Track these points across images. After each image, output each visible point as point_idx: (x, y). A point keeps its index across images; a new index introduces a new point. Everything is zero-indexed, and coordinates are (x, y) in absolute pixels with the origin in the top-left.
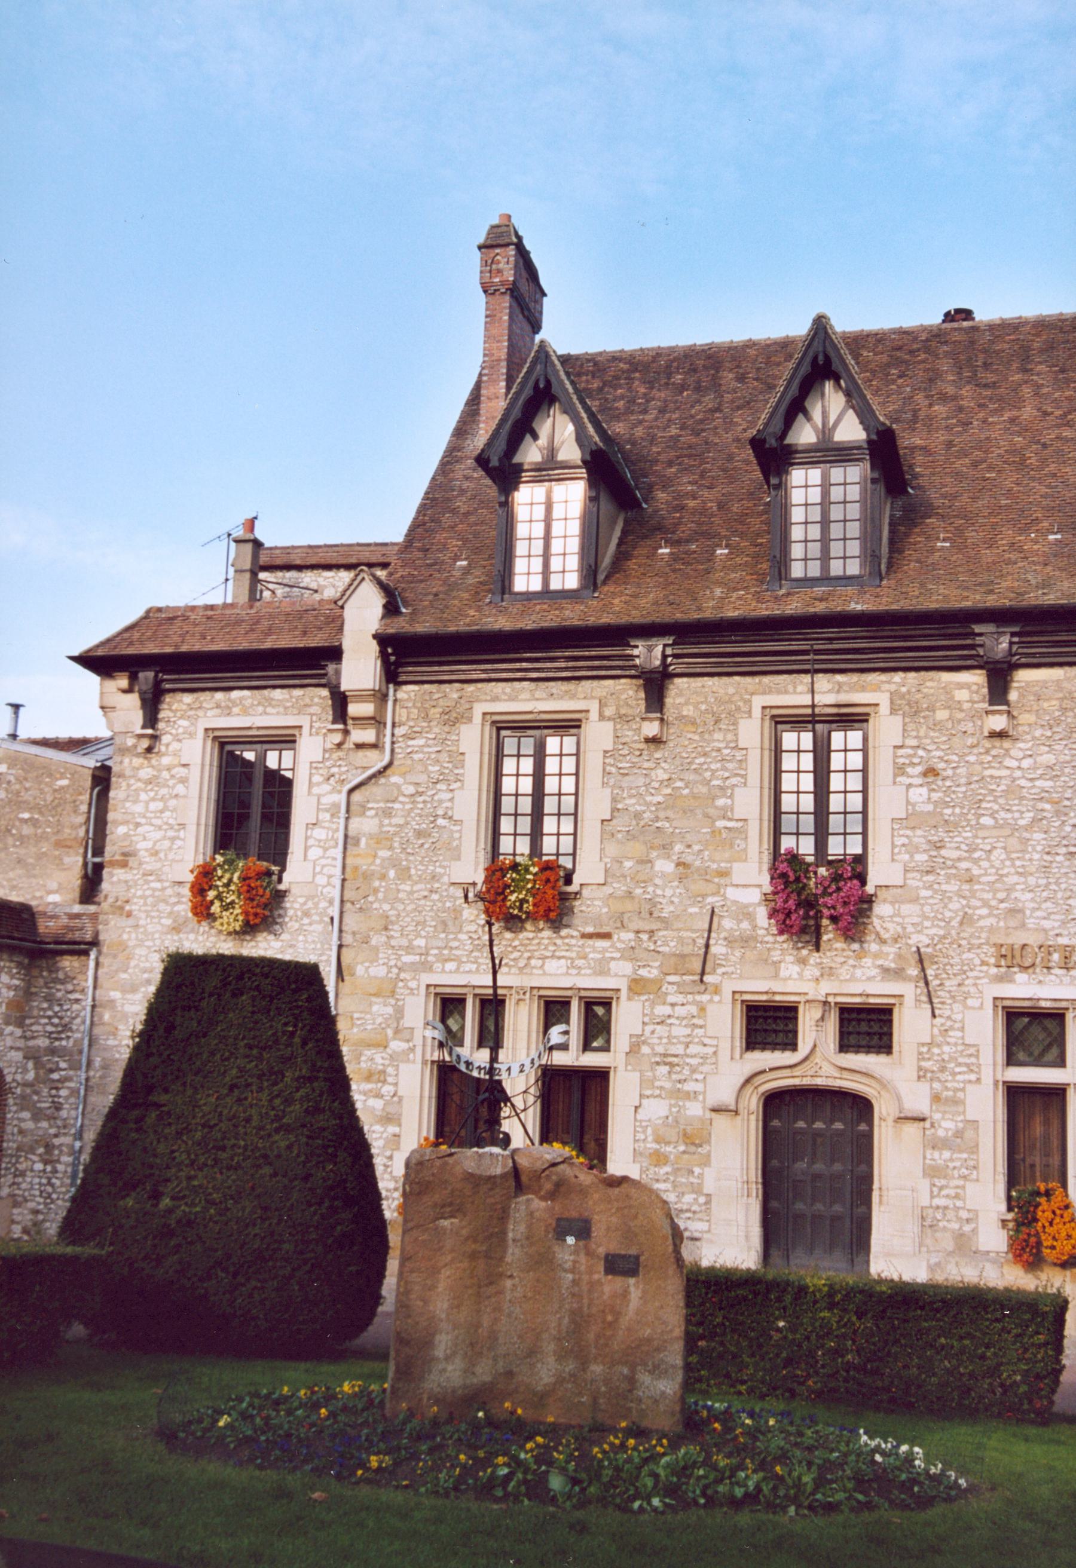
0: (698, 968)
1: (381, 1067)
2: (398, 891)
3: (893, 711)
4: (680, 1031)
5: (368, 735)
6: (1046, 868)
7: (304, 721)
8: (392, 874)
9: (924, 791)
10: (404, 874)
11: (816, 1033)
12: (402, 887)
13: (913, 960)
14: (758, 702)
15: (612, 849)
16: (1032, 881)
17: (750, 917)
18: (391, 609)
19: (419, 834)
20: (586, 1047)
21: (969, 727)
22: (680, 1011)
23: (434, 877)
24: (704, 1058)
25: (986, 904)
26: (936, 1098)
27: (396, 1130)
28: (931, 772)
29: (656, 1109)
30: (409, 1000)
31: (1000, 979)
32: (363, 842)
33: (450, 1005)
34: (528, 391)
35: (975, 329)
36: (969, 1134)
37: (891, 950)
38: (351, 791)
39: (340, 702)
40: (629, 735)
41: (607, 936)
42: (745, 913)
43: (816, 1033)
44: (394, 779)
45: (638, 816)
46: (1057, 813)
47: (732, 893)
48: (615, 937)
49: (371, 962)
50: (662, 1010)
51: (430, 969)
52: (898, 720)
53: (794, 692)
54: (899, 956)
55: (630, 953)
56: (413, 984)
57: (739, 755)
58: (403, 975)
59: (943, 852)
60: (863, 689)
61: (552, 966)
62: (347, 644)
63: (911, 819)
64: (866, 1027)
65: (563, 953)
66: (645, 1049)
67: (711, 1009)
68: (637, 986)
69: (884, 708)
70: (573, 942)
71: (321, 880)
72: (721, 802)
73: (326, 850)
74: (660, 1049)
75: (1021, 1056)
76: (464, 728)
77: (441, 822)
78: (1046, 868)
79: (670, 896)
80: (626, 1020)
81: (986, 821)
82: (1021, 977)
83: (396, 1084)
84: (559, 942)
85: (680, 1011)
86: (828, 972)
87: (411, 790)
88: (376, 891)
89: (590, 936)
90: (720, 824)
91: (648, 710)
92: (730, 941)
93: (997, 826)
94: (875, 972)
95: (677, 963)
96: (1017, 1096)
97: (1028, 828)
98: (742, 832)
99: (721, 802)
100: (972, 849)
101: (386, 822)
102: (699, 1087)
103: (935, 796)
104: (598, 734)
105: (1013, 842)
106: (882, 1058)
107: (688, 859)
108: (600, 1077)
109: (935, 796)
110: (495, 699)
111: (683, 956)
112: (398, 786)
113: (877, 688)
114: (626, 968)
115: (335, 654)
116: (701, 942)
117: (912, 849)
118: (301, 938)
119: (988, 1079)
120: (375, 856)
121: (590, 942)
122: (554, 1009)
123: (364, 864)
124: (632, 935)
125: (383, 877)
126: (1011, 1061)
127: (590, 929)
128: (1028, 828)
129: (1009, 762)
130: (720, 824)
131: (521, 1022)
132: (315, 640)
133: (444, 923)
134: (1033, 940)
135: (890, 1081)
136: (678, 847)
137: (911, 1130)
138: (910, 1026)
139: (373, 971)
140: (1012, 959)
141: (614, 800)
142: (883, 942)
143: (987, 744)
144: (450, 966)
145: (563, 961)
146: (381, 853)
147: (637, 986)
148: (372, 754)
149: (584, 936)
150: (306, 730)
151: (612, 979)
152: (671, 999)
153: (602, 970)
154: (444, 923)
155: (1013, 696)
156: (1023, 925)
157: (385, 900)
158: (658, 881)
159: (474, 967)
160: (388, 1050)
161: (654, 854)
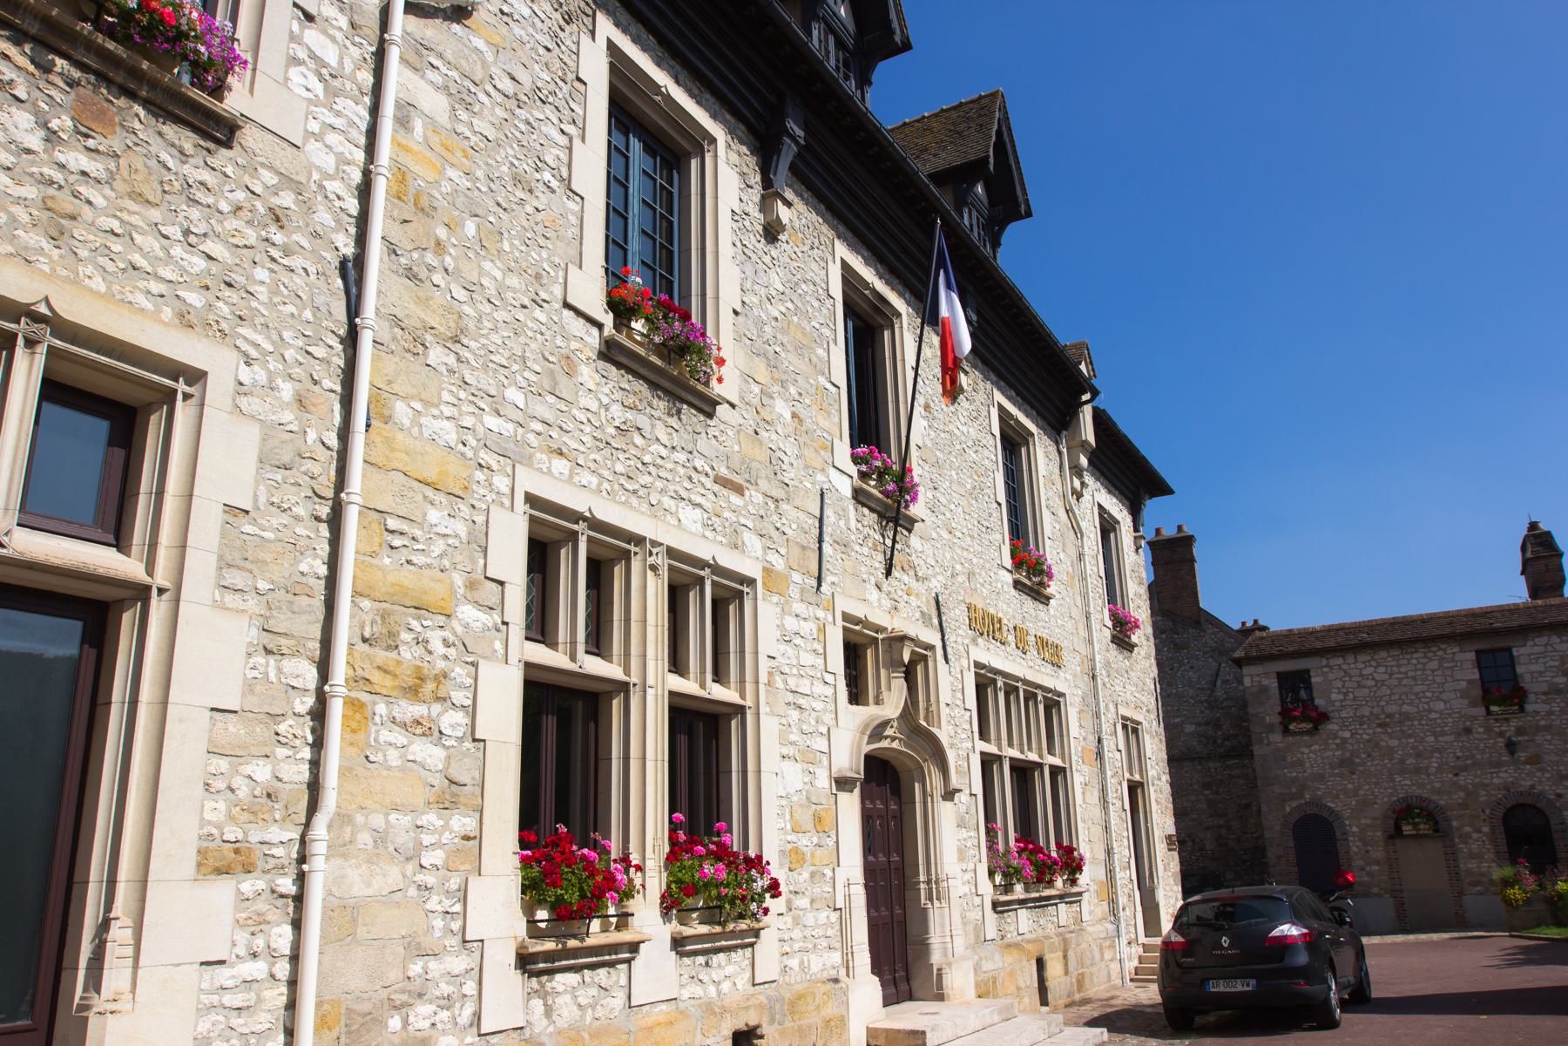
1: (441, 665)
8: (470, 228)
12: (487, 265)
19: (517, 180)
30: (496, 512)
32: (418, 125)
41: (739, 490)
48: (747, 493)
51: (528, 461)
58: (487, 457)
61: (690, 516)
65: (699, 499)
73: (333, 94)
74: (792, 682)
77: (547, 176)
83: (472, 711)
84: (694, 475)
94: (918, 615)
101: (463, 115)
102: (821, 744)
107: (799, 408)
118: (261, 274)
120: (442, 172)
121: (725, 492)
123: (422, 172)
127: (723, 471)
139: (431, 424)
144: (560, 465)
145: (698, 511)
146: (451, 173)
149: (719, 480)
159: (594, 480)
160: (455, 623)
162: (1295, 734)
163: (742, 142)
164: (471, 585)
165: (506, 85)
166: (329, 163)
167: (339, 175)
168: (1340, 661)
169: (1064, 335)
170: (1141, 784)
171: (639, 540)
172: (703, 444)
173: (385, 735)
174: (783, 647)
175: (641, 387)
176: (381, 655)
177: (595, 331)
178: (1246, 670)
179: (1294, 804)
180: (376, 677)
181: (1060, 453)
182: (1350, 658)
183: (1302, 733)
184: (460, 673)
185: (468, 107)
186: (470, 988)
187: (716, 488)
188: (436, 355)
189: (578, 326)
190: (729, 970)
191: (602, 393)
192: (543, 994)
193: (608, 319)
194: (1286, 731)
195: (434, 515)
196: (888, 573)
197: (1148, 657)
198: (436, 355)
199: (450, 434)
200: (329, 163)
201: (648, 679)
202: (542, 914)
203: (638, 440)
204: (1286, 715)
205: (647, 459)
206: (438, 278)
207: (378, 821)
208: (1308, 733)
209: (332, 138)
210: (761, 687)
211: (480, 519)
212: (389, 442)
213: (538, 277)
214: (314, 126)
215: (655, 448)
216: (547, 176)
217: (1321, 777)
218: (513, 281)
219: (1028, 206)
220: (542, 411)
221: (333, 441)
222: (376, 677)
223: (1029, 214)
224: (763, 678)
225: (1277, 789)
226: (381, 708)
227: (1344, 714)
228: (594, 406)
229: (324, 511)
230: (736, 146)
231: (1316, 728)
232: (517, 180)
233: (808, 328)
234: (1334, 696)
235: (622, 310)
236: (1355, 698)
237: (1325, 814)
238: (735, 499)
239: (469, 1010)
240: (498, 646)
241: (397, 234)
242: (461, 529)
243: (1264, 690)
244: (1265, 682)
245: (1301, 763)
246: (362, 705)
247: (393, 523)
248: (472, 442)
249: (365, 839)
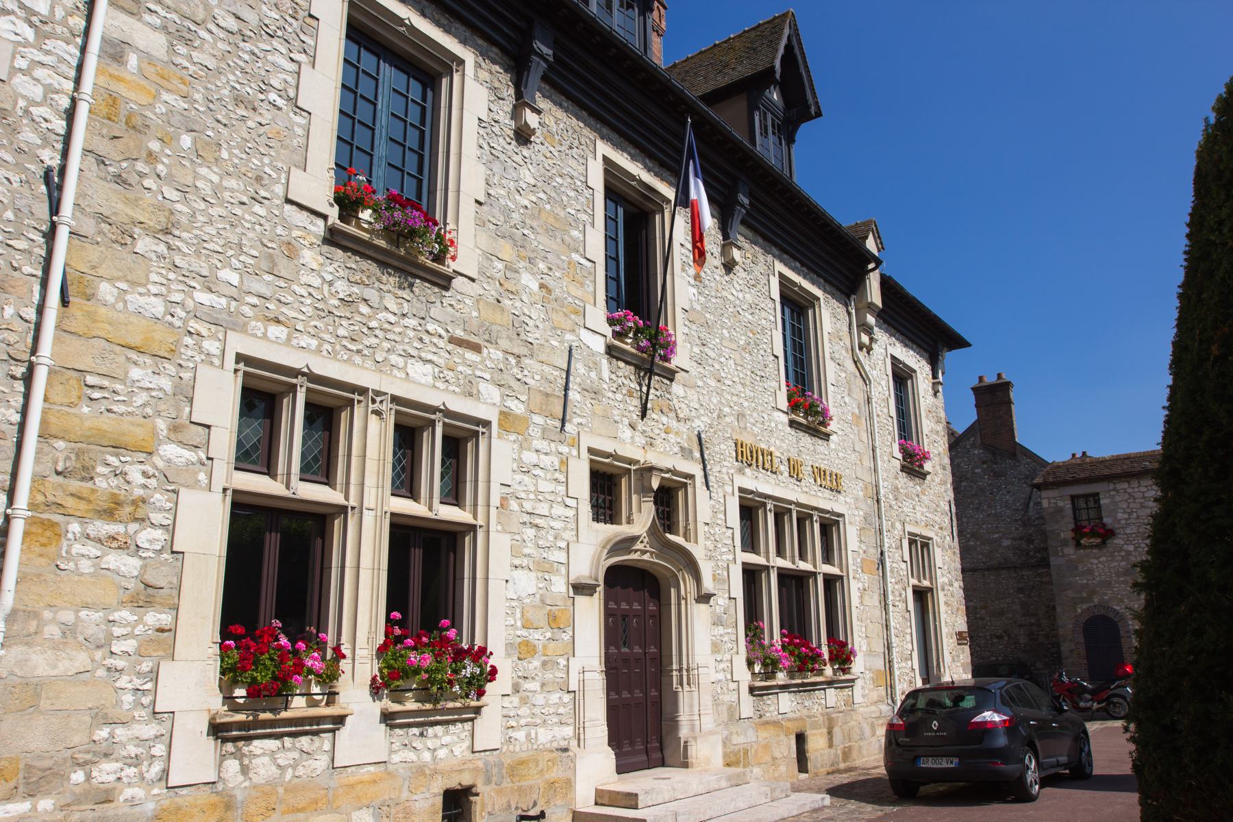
1: (139, 492)
2: (196, 176)
8: (186, 141)
9: (695, 291)
10: (205, 152)
12: (203, 171)
17: (596, 366)
19: (239, 100)
22: (546, 461)
23: (259, 179)
27: (166, 619)
30: (203, 370)
32: (133, 60)
33: (261, 398)
41: (477, 348)
45: (507, 212)
48: (485, 351)
49: (133, 283)
51: (243, 329)
56: (212, 346)
58: (194, 325)
59: (706, 350)
61: (418, 370)
65: (430, 357)
70: (441, 343)
74: (528, 506)
77: (273, 96)
80: (499, 460)
83: (171, 529)
84: (426, 338)
85: (546, 461)
89: (460, 342)
94: (676, 449)
99: (575, 233)
101: (182, 49)
102: (562, 557)
107: (549, 281)
120: (156, 97)
121: (460, 350)
123: (133, 99)
124: (500, 355)
127: (459, 333)
131: (370, 440)
144: (275, 331)
145: (429, 366)
146: (166, 96)
149: (453, 340)
157: (169, 179)
158: (525, 298)
159: (314, 343)
160: (156, 460)
161: (522, 264)
162: (1085, 547)
163: (494, 62)
164: (175, 429)
165: (232, 24)
166: (37, 92)
167: (45, 101)
168: (1126, 485)
169: (844, 216)
170: (931, 590)
171: (363, 391)
172: (435, 311)
173: (77, 548)
174: (519, 477)
175: (373, 267)
176: (74, 485)
177: (320, 222)
178: (1045, 494)
179: (1085, 606)
180: (70, 502)
181: (849, 314)
182: (1135, 483)
183: (1092, 547)
184: (159, 498)
185: (188, 42)
186: (159, 750)
187: (450, 347)
188: (144, 244)
189: (302, 218)
190: (447, 739)
191: (323, 272)
192: (238, 755)
193: (333, 213)
194: (1078, 545)
195: (135, 373)
196: (643, 415)
197: (943, 483)
198: (144, 244)
199: (158, 308)
200: (37, 92)
201: (368, 503)
202: (240, 692)
203: (364, 309)
204: (1078, 531)
205: (373, 324)
206: (147, 183)
207: (68, 616)
208: (1097, 546)
209: (39, 73)
210: (493, 511)
211: (187, 375)
212: (92, 317)
213: (259, 179)
214: (21, 63)
215: (382, 315)
216: (273, 96)
217: (1108, 584)
218: (232, 183)
219: (818, 107)
220: (257, 287)
221: (31, 314)
222: (70, 502)
223: (819, 114)
224: (495, 501)
225: (1070, 594)
226: (75, 527)
227: (1128, 531)
228: (316, 282)
229: (20, 370)
230: (486, 65)
231: (1104, 543)
232: (239, 100)
233: (562, 214)
234: (1120, 515)
235: (348, 204)
236: (1138, 517)
237: (1111, 615)
238: (471, 356)
239: (157, 768)
240: (202, 477)
241: (104, 147)
242: (166, 384)
243: (1060, 510)
244: (1061, 504)
245: (1090, 572)
246: (53, 525)
247: (91, 380)
248: (180, 312)
249: (52, 631)
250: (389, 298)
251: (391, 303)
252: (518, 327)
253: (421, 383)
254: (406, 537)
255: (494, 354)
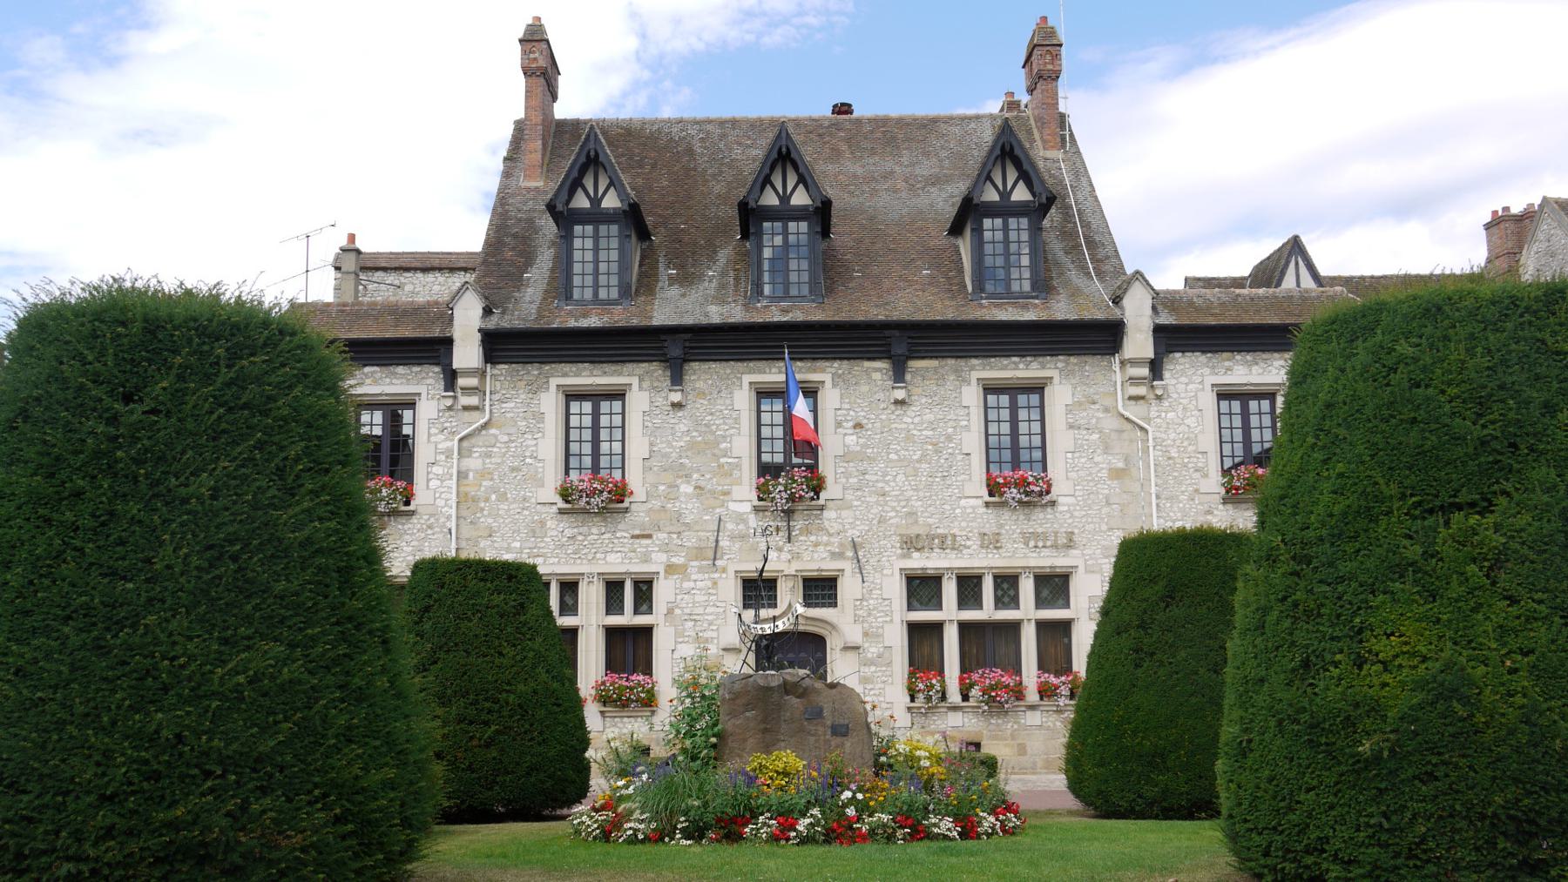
0: (711, 554)
3: (834, 386)
4: (700, 598)
5: (473, 400)
6: (929, 486)
7: (422, 389)
8: (493, 497)
10: (503, 497)
11: (789, 596)
13: (850, 546)
14: (747, 379)
15: (651, 478)
16: (921, 494)
17: (745, 521)
18: (487, 312)
19: (513, 469)
20: (636, 612)
21: (881, 396)
24: (717, 614)
25: (893, 509)
26: (866, 634)
28: (858, 426)
29: (688, 650)
31: (904, 556)
32: (471, 475)
34: (583, 159)
35: (859, 121)
36: (887, 655)
37: (835, 540)
38: (461, 440)
39: (451, 377)
40: (660, 401)
41: (649, 536)
42: (741, 519)
43: (789, 596)
44: (493, 431)
45: (666, 455)
46: (936, 452)
47: (732, 506)
50: (686, 585)
52: (837, 392)
53: (773, 375)
54: (841, 545)
55: (665, 548)
57: (735, 415)
60: (815, 371)
61: (611, 558)
62: (457, 334)
63: (847, 456)
64: (821, 589)
66: (678, 611)
67: (720, 583)
68: (671, 569)
69: (828, 384)
71: (440, 503)
72: (723, 446)
74: (687, 611)
75: (915, 603)
76: (543, 396)
78: (929, 486)
79: (690, 508)
80: (663, 593)
81: (893, 456)
82: (916, 555)
86: (796, 556)
87: (506, 438)
88: (482, 510)
89: (637, 537)
90: (723, 460)
91: (673, 383)
92: (732, 538)
93: (900, 460)
95: (698, 553)
96: (914, 629)
97: (919, 461)
98: (738, 466)
99: (723, 446)
100: (884, 475)
102: (714, 634)
103: (861, 441)
104: (638, 400)
105: (910, 470)
106: (831, 610)
107: (702, 484)
108: (647, 631)
109: (861, 441)
110: (565, 375)
111: (700, 549)
112: (495, 436)
113: (823, 371)
114: (663, 557)
115: (448, 342)
116: (713, 539)
117: (847, 475)
119: (897, 618)
122: (613, 588)
123: (472, 491)
125: (487, 500)
126: (910, 608)
127: (637, 532)
128: (919, 461)
129: (906, 419)
130: (723, 460)
131: (591, 597)
132: (436, 333)
133: (534, 531)
134: (922, 531)
135: (840, 622)
136: (695, 476)
137: (851, 655)
138: (848, 589)
140: (911, 544)
141: (651, 444)
142: (830, 535)
143: (893, 407)
147: (671, 569)
148: (476, 414)
149: (633, 537)
150: (424, 396)
151: (655, 564)
152: (694, 577)
153: (646, 559)
154: (534, 531)
155: (908, 377)
156: (916, 522)
157: (489, 515)
165: (506, 438)
191: (560, 528)
233: (711, 438)
238: (645, 542)
250: (595, 531)
251: (594, 530)
252: (679, 516)
253: (616, 564)
254: (614, 635)
255: (660, 536)
